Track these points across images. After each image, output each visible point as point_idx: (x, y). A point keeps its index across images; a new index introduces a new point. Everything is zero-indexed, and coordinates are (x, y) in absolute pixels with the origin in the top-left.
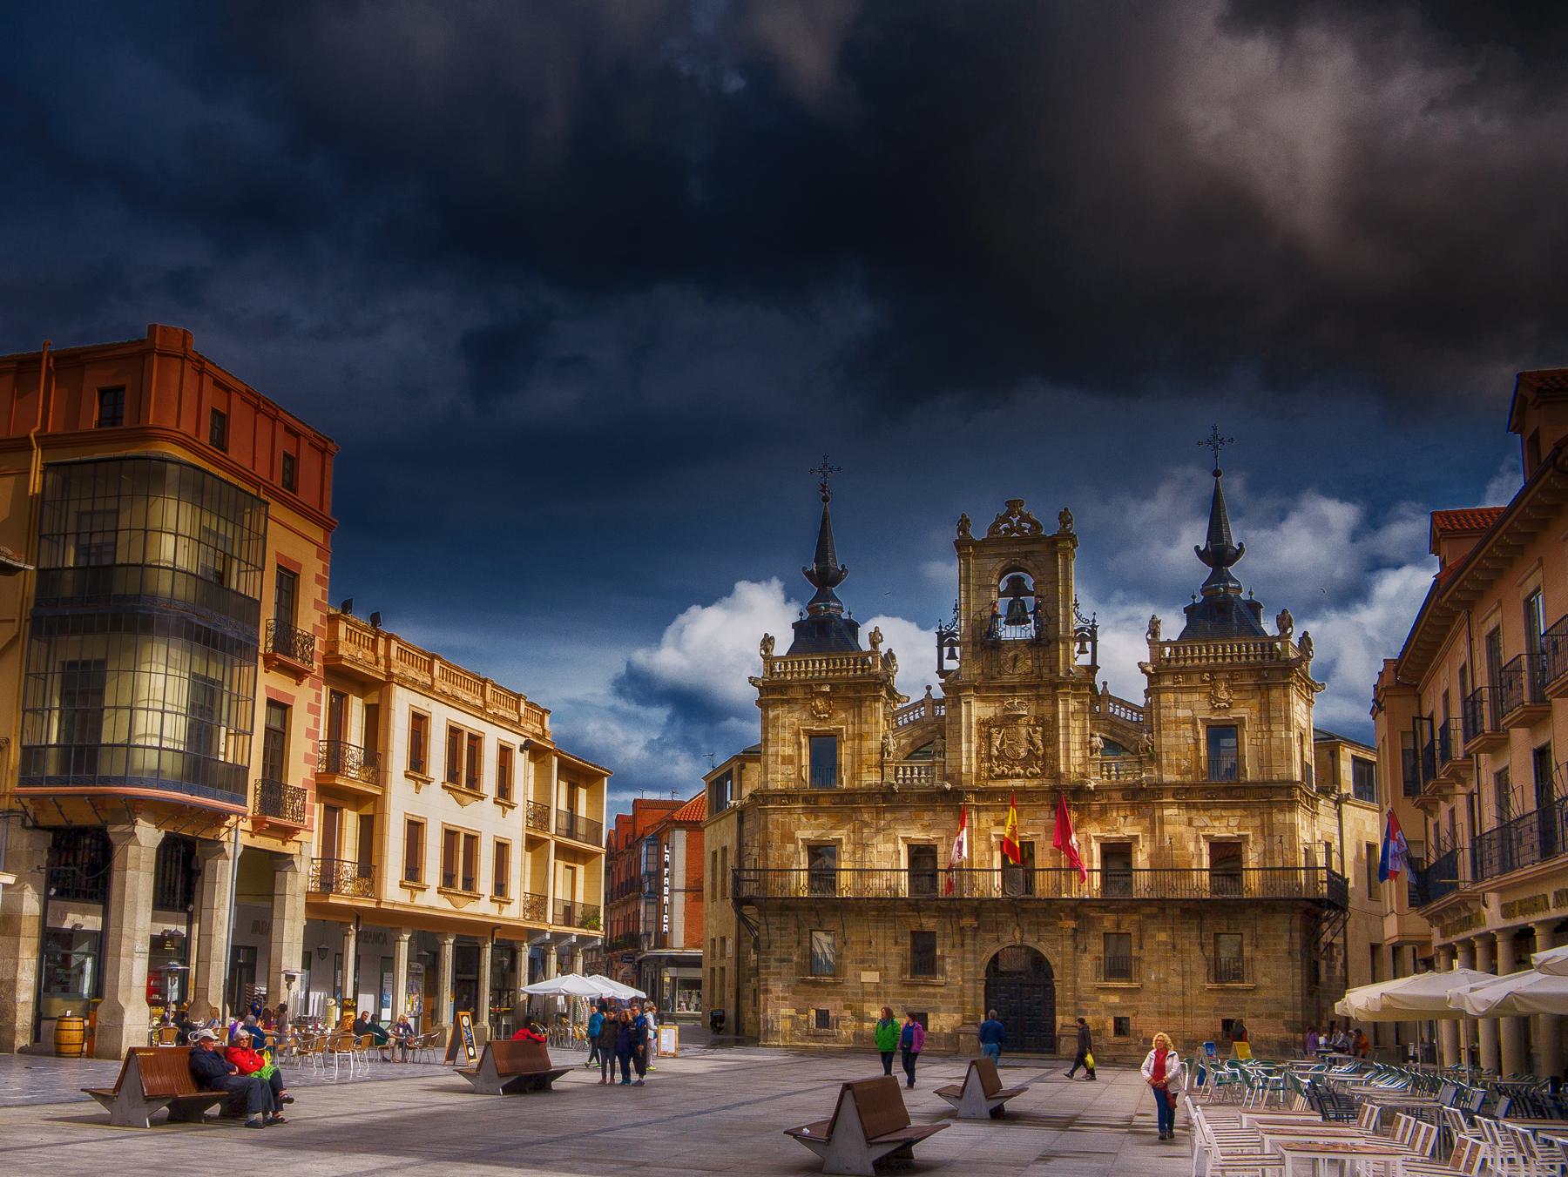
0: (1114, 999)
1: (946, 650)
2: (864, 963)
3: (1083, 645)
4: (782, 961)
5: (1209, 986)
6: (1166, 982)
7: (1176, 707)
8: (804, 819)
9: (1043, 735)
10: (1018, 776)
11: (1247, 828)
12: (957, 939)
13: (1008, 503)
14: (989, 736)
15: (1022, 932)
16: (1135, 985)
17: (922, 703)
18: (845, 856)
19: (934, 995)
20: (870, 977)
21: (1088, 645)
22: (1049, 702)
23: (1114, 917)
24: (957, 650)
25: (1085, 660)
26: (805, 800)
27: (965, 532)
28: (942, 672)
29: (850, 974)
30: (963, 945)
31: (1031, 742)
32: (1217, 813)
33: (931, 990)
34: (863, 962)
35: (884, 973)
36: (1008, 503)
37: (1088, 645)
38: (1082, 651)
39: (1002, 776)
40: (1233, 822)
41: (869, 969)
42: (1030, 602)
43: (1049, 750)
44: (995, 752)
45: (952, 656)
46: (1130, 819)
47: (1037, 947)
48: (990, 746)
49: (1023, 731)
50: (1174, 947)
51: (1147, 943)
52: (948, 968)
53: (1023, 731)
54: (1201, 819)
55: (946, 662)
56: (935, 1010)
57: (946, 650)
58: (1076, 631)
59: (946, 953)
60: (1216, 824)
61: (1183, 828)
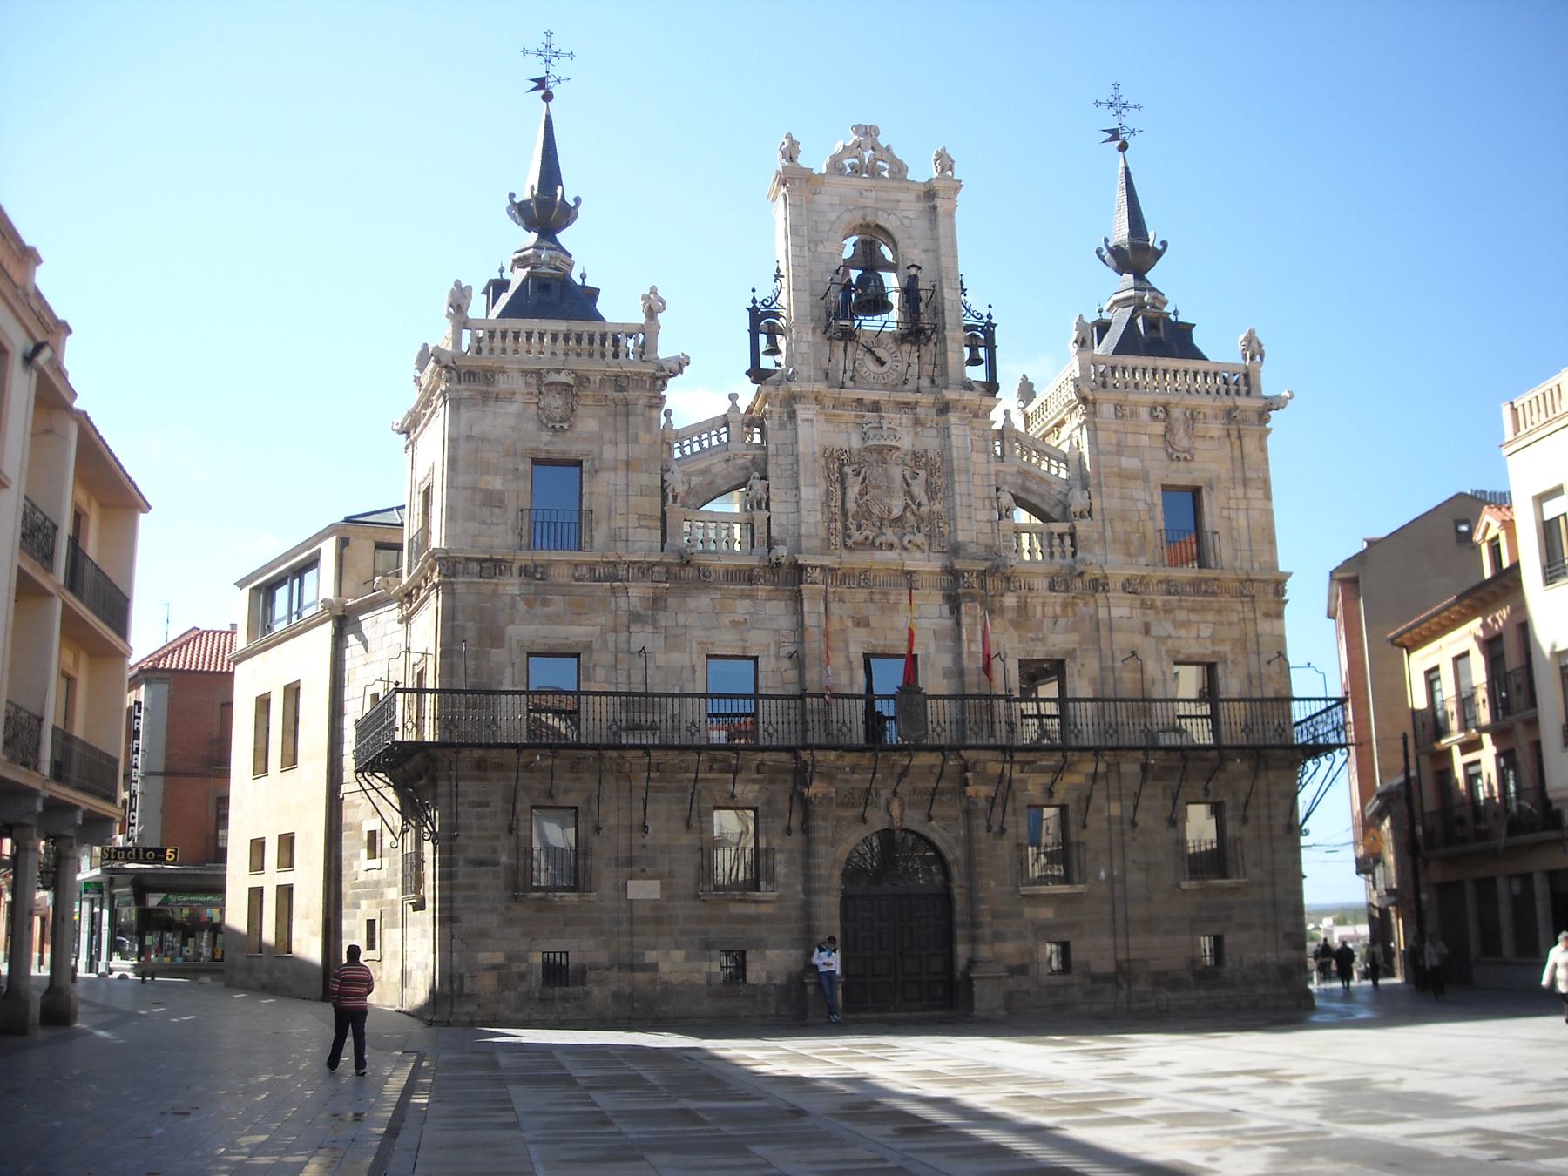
0: (1047, 913)
1: (763, 338)
2: (632, 864)
3: (973, 350)
4: (481, 863)
5: (1185, 885)
6: (1123, 881)
7: (1119, 453)
8: (522, 606)
9: (928, 485)
10: (891, 546)
11: (1222, 640)
12: (795, 823)
13: (857, 128)
14: (842, 479)
15: (902, 804)
16: (1080, 888)
17: (725, 421)
18: (600, 674)
19: (756, 919)
20: (644, 890)
21: (982, 352)
22: (933, 432)
23: (1046, 779)
24: (782, 343)
25: (977, 374)
26: (524, 571)
27: (791, 159)
28: (757, 374)
29: (606, 878)
30: (806, 829)
31: (909, 494)
32: (1181, 615)
33: (751, 909)
34: (630, 862)
35: (667, 878)
36: (857, 128)
37: (982, 352)
38: (975, 361)
39: (869, 545)
40: (1205, 631)
41: (644, 875)
42: (891, 280)
43: (937, 507)
44: (851, 506)
45: (774, 351)
46: (1062, 622)
47: (924, 831)
48: (844, 493)
49: (897, 473)
50: (1134, 824)
51: (1092, 821)
52: (780, 870)
53: (897, 473)
54: (1163, 627)
55: (762, 357)
56: (760, 945)
57: (763, 338)
58: (967, 328)
59: (776, 843)
60: (1183, 633)
61: (1138, 640)
